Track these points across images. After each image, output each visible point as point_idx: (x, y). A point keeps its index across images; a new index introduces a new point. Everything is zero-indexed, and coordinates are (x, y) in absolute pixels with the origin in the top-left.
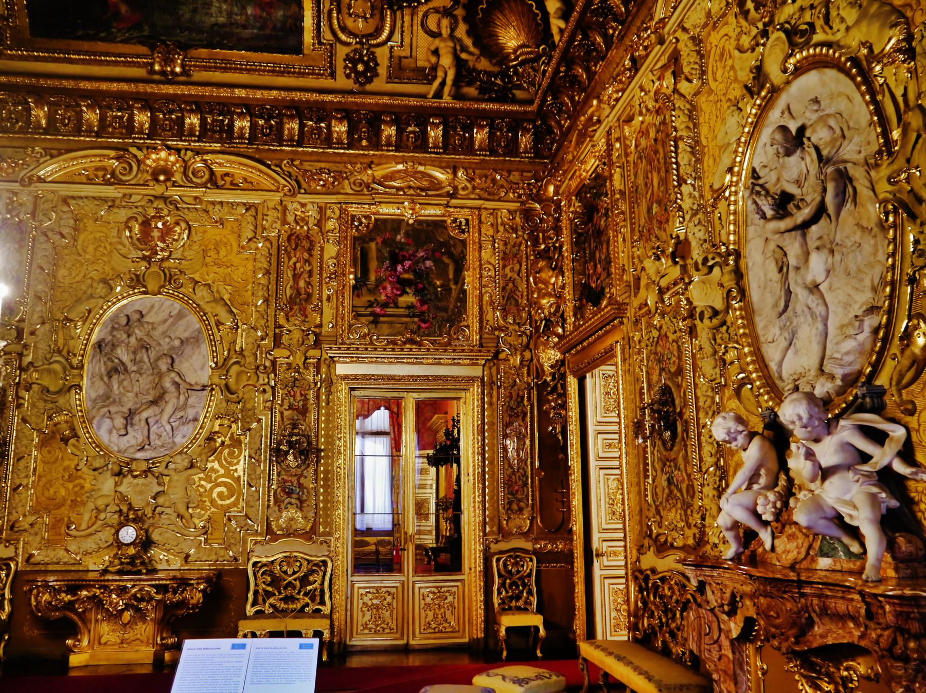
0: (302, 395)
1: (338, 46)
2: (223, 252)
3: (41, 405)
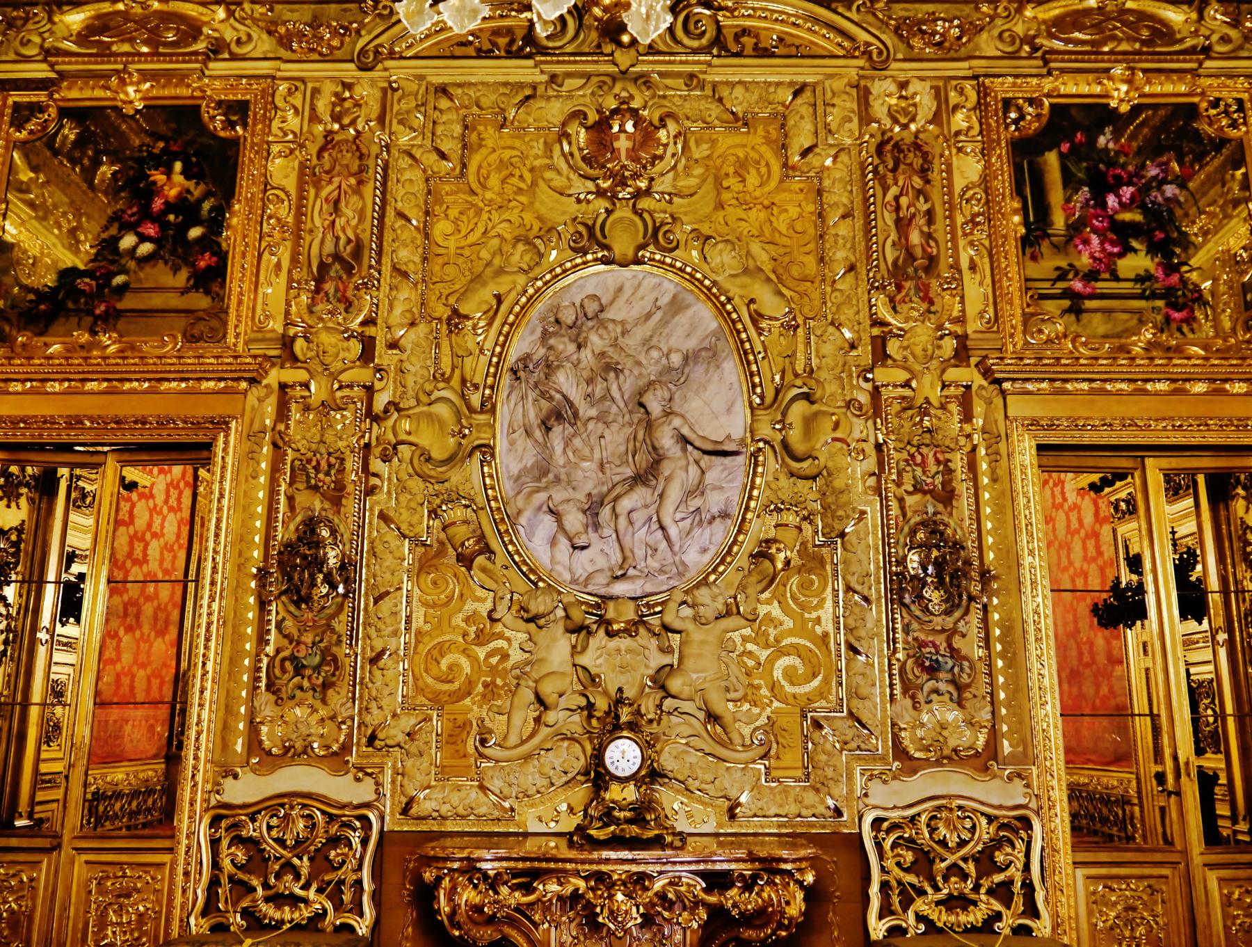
0: (938, 462)
2: (752, 179)
3: (416, 484)
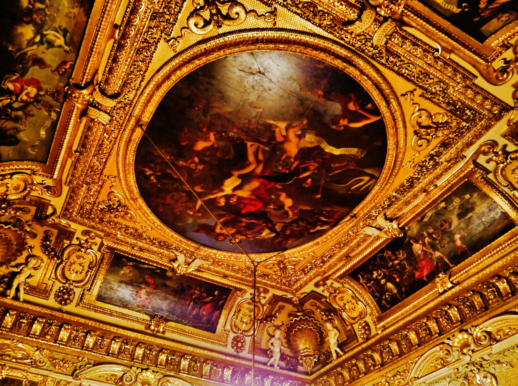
1: (231, 332)
